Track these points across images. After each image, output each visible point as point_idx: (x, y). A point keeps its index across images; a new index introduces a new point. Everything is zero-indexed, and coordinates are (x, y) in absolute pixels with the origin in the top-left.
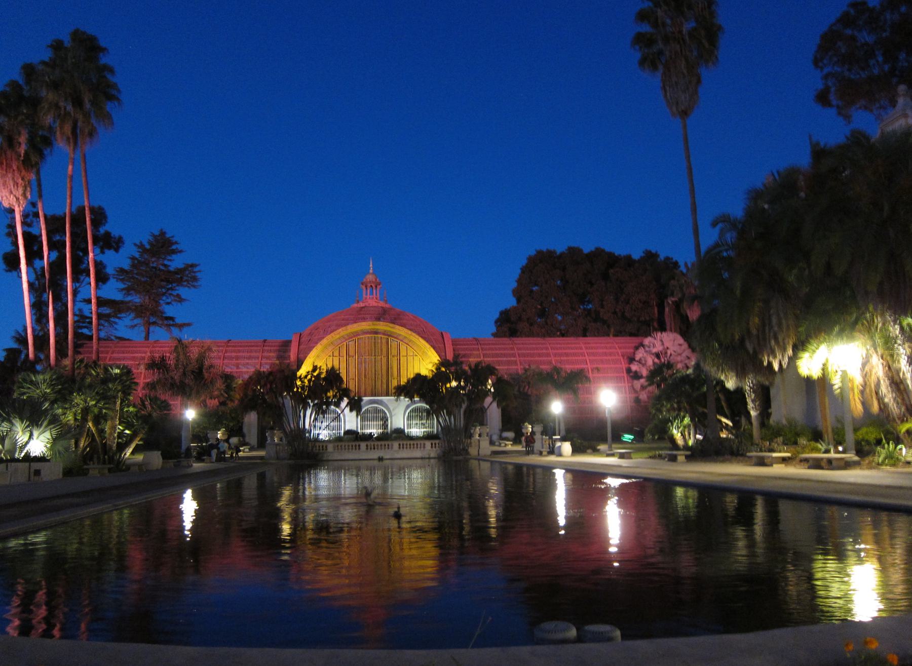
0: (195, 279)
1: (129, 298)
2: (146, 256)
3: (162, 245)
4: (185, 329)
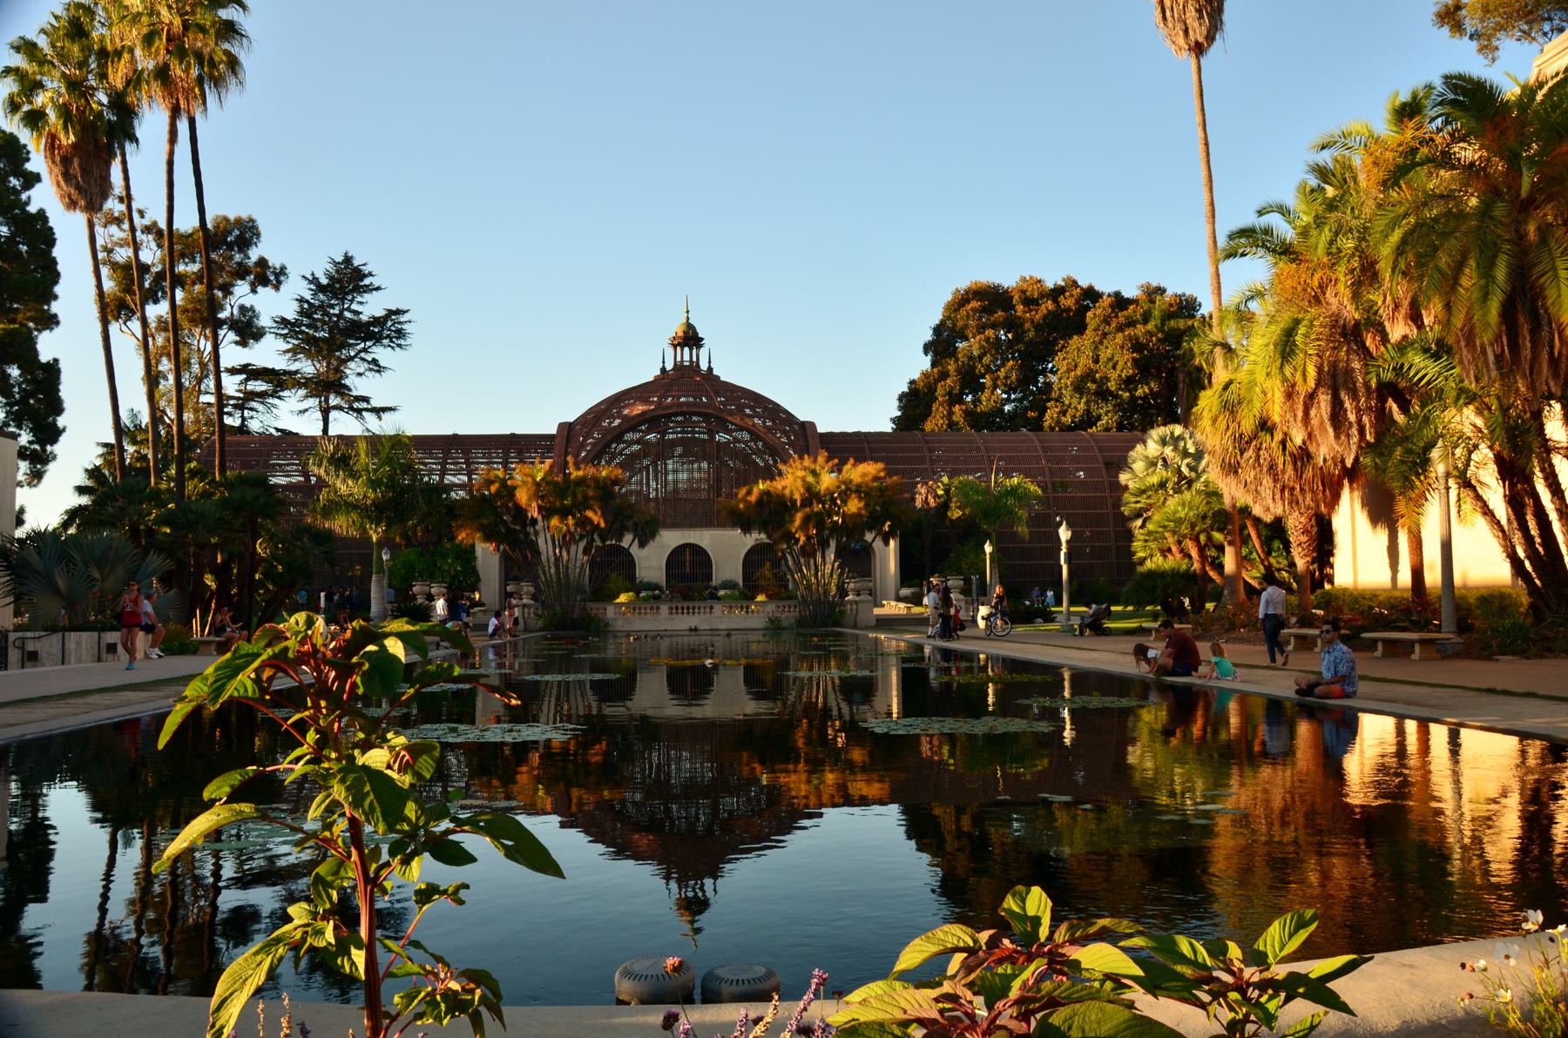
0: (400, 334)
1: (293, 368)
3: (348, 279)
4: (386, 416)
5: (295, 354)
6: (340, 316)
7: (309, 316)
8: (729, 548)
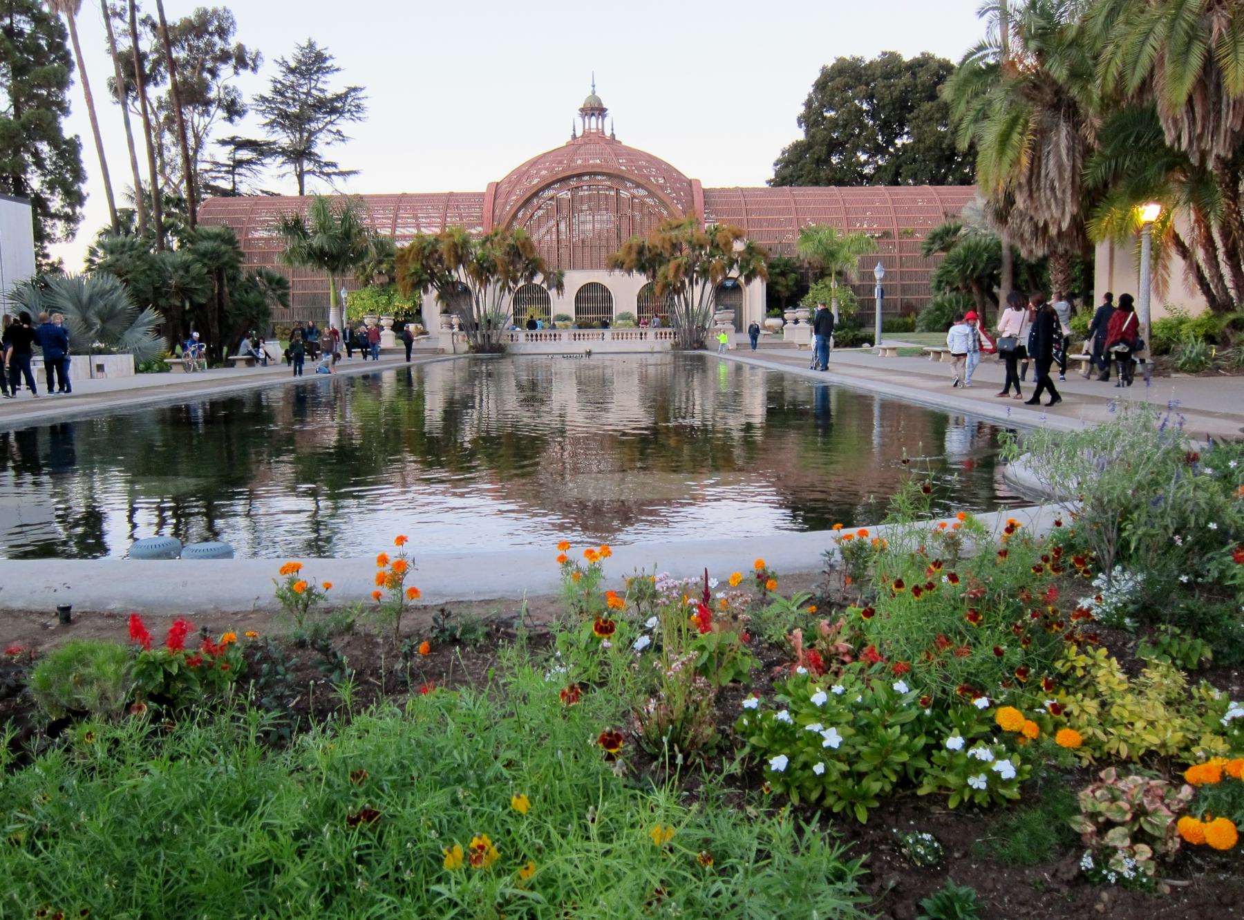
1: (271, 139)
2: (291, 77)
3: (313, 63)
4: (352, 178)
5: (273, 127)
6: (308, 94)
7: (282, 94)
8: (626, 289)
